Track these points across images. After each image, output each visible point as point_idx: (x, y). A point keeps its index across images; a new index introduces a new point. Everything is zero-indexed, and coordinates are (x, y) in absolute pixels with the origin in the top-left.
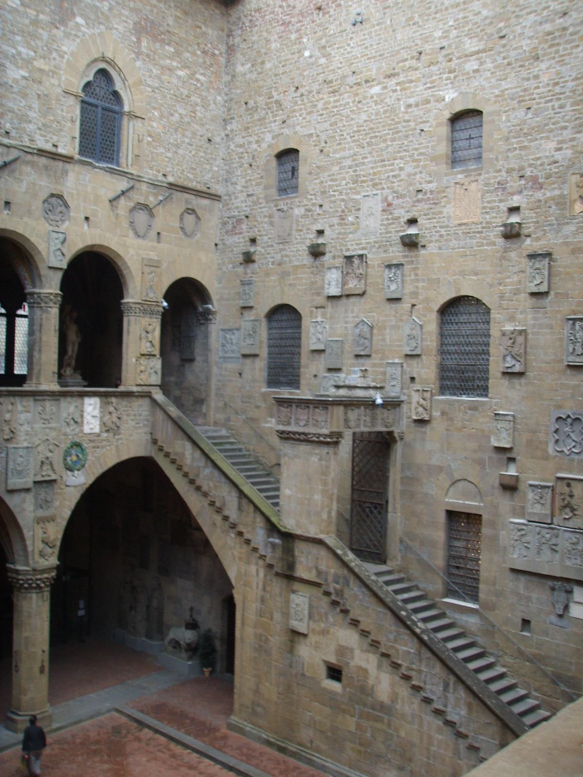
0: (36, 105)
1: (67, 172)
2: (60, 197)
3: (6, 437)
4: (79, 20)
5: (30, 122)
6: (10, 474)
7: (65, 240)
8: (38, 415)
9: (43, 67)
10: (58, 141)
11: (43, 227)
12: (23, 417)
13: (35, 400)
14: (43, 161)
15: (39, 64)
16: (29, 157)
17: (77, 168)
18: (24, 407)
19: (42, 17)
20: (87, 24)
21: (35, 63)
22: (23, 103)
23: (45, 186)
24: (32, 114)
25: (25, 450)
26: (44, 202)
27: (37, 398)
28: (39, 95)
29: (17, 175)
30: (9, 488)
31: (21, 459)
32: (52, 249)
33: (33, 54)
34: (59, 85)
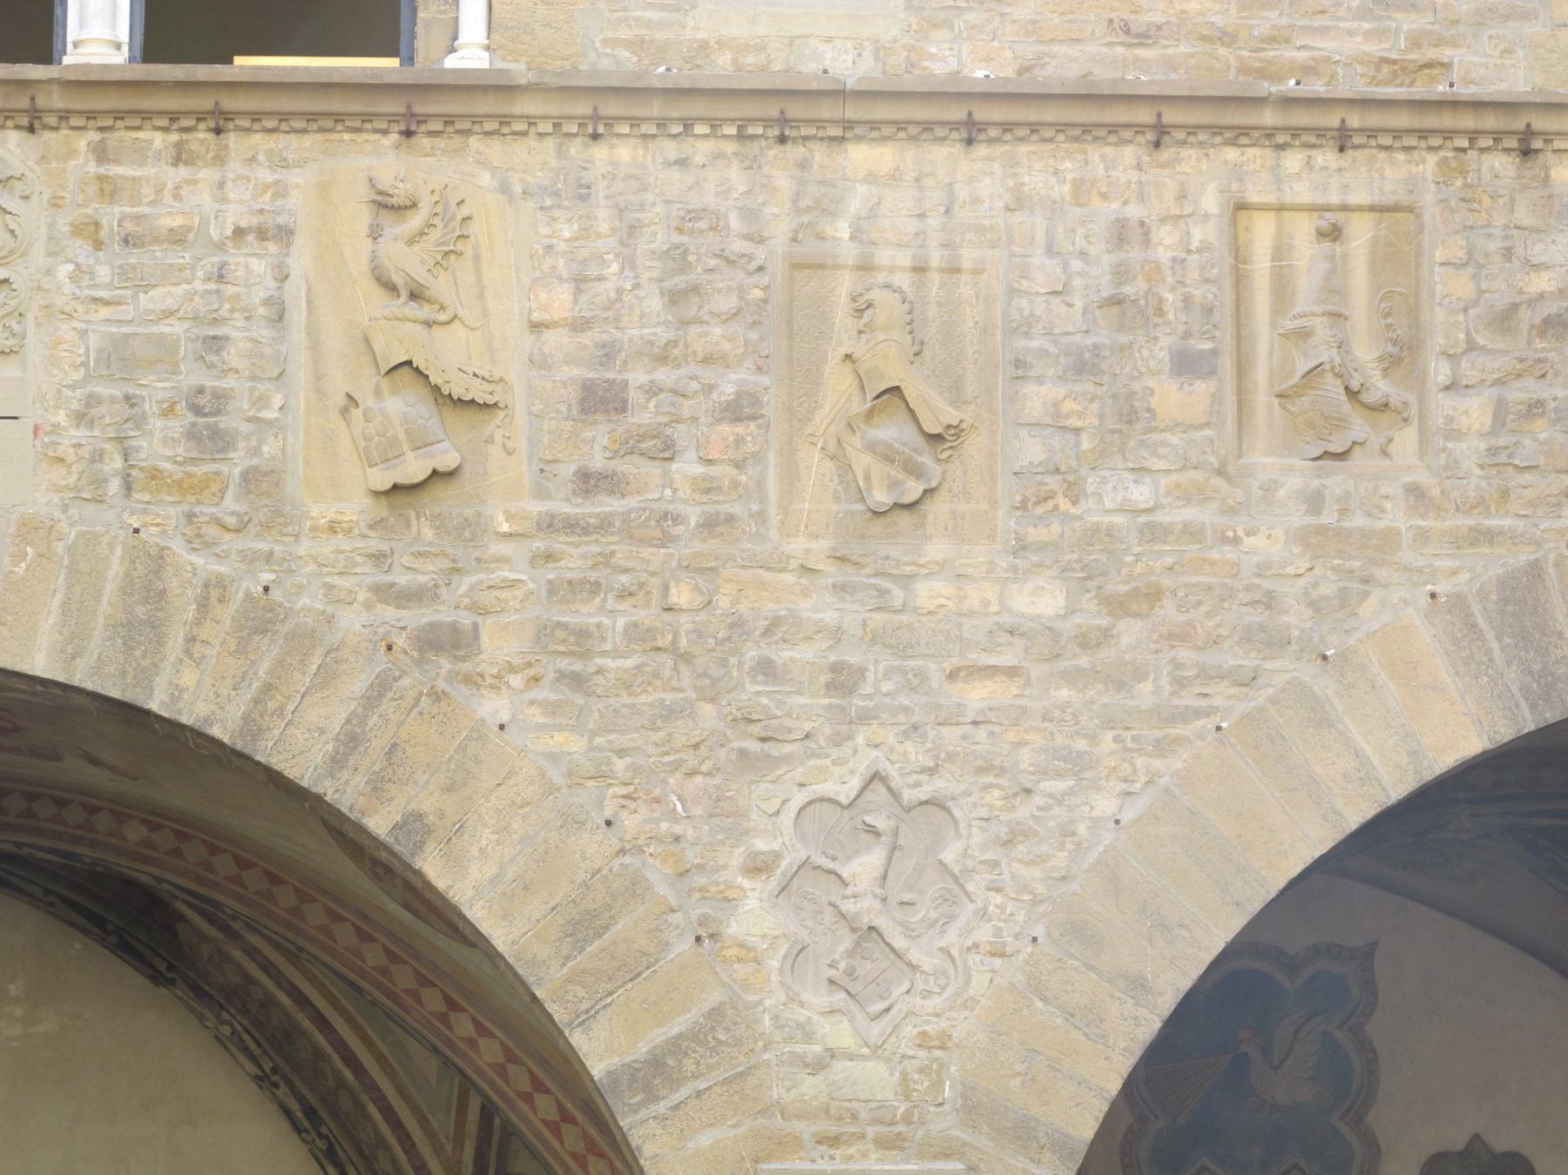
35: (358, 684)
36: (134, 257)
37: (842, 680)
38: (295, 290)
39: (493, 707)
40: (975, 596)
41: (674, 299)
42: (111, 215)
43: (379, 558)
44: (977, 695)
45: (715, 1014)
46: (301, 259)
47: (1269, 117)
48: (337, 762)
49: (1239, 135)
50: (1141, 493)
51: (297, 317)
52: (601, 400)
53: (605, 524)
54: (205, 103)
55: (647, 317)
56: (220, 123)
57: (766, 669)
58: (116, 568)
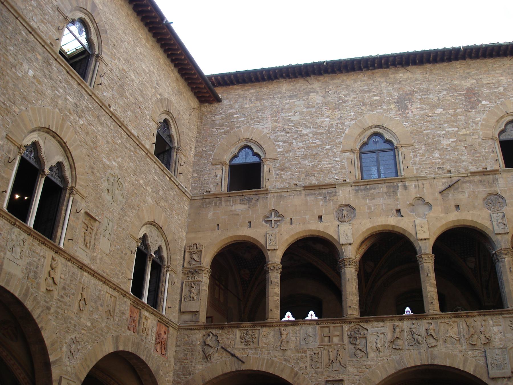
0: (465, 152)
1: (497, 180)
2: (497, 194)
3: (483, 343)
4: (484, 103)
5: (463, 161)
6: (490, 367)
7: (504, 216)
8: (509, 327)
9: (465, 133)
10: (486, 165)
11: (486, 212)
12: (496, 329)
13: (504, 317)
14: (477, 178)
15: (464, 132)
16: (467, 179)
17: (504, 175)
18: (495, 322)
19: (458, 110)
20: (490, 102)
21: (459, 133)
22: (456, 153)
23: (482, 191)
24: (463, 158)
25: (500, 350)
26: (484, 200)
27: (505, 316)
28: (466, 147)
29: (460, 190)
30: (491, 377)
31: (498, 357)
32: (495, 223)
33: (457, 129)
34: (479, 138)
35: (41, 309)
36: (34, 254)
37: (75, 326)
38: (44, 264)
39: (50, 317)
40: (85, 321)
41: (71, 281)
42: (33, 248)
43: (45, 297)
44: (83, 332)
45: (60, 358)
46: (46, 261)
47: (111, 284)
48: (38, 317)
49: (108, 285)
50: (97, 317)
51: (44, 267)
52: (64, 288)
53: (61, 302)
54: (43, 240)
55: (68, 282)
56: (43, 243)
57: (70, 322)
58: (25, 287)
